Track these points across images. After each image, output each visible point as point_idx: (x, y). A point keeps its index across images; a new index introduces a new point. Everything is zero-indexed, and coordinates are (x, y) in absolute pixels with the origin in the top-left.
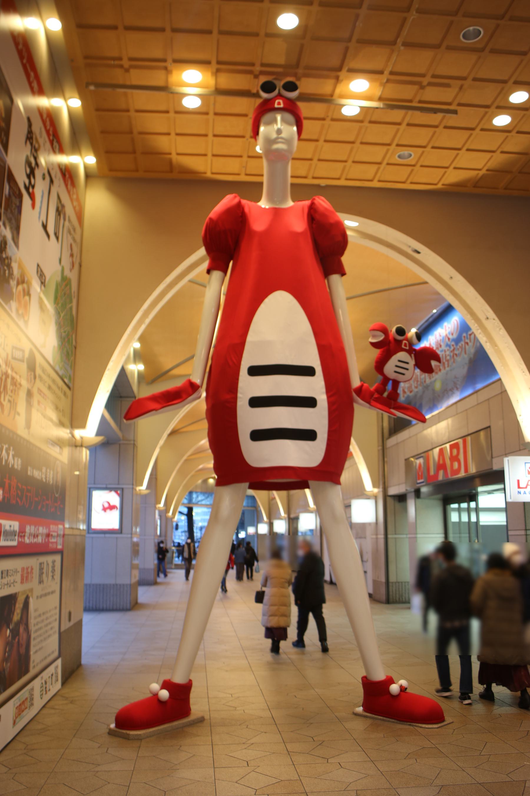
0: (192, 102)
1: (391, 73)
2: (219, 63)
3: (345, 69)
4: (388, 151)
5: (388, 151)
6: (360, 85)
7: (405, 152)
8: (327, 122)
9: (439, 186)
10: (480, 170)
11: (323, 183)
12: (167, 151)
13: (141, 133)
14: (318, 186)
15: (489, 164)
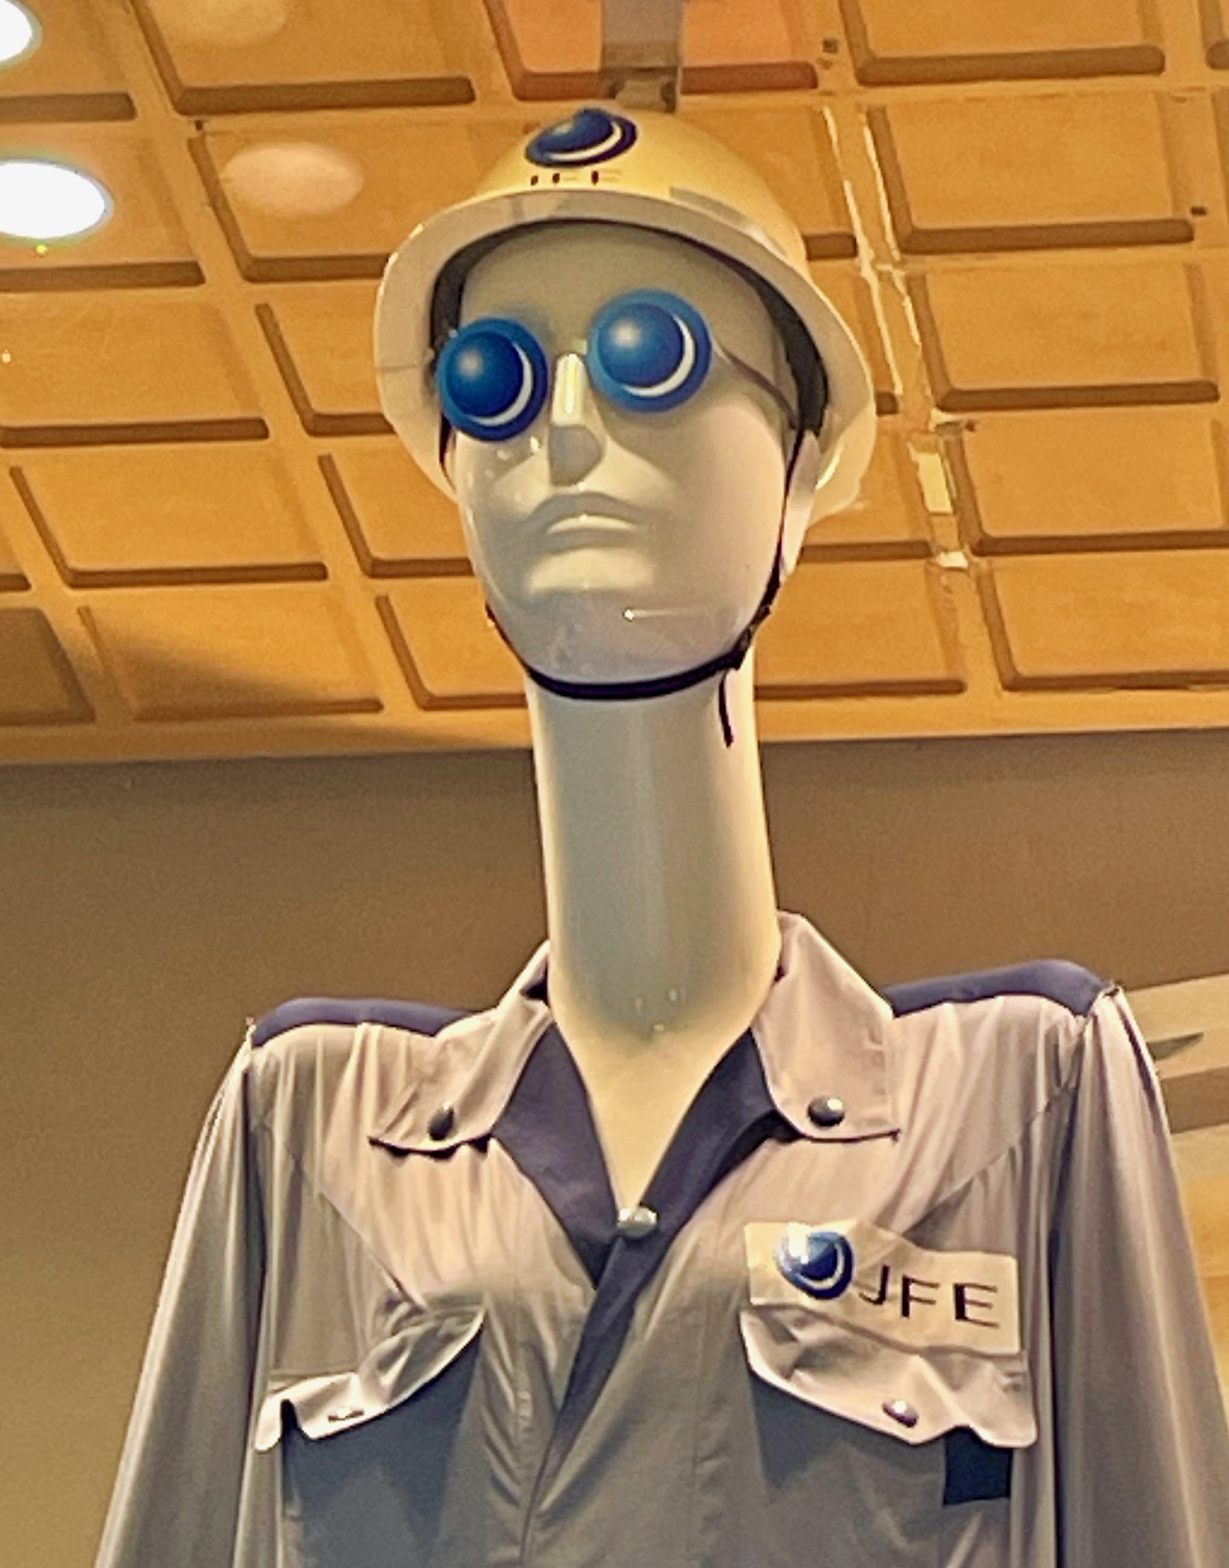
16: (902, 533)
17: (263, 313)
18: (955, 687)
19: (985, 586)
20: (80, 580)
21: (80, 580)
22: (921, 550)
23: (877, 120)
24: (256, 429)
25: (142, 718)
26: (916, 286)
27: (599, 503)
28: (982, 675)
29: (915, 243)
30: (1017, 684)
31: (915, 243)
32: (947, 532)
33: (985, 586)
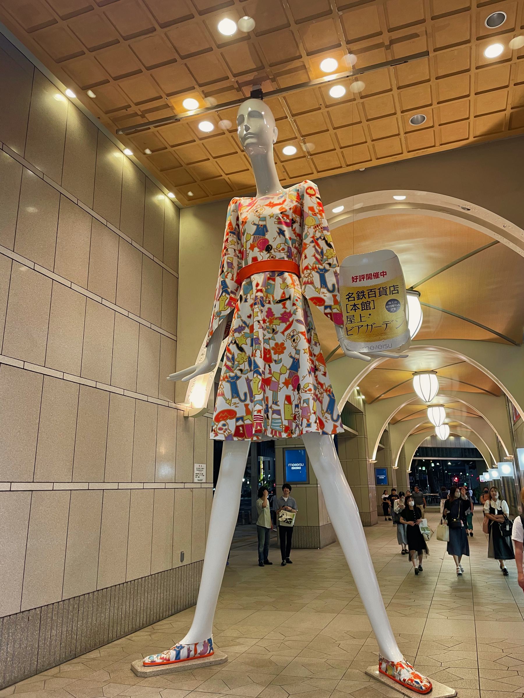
0: (206, 127)
1: (348, 42)
2: (200, 85)
3: (304, 53)
4: (397, 119)
5: (397, 119)
6: (329, 66)
7: (417, 115)
8: (324, 110)
9: (471, 139)
10: (504, 110)
11: (362, 167)
12: (219, 175)
13: (188, 164)
14: (358, 171)
15: (510, 102)
16: (302, 155)
17: (232, 137)
18: (313, 173)
19: (312, 159)
20: (227, 174)
21: (227, 174)
22: (304, 157)
23: (284, 98)
24: (237, 153)
25: (239, 190)
26: (295, 121)
27: (250, 133)
28: (315, 172)
29: (293, 115)
30: (318, 172)
31: (293, 115)
32: (307, 154)
33: (312, 159)
